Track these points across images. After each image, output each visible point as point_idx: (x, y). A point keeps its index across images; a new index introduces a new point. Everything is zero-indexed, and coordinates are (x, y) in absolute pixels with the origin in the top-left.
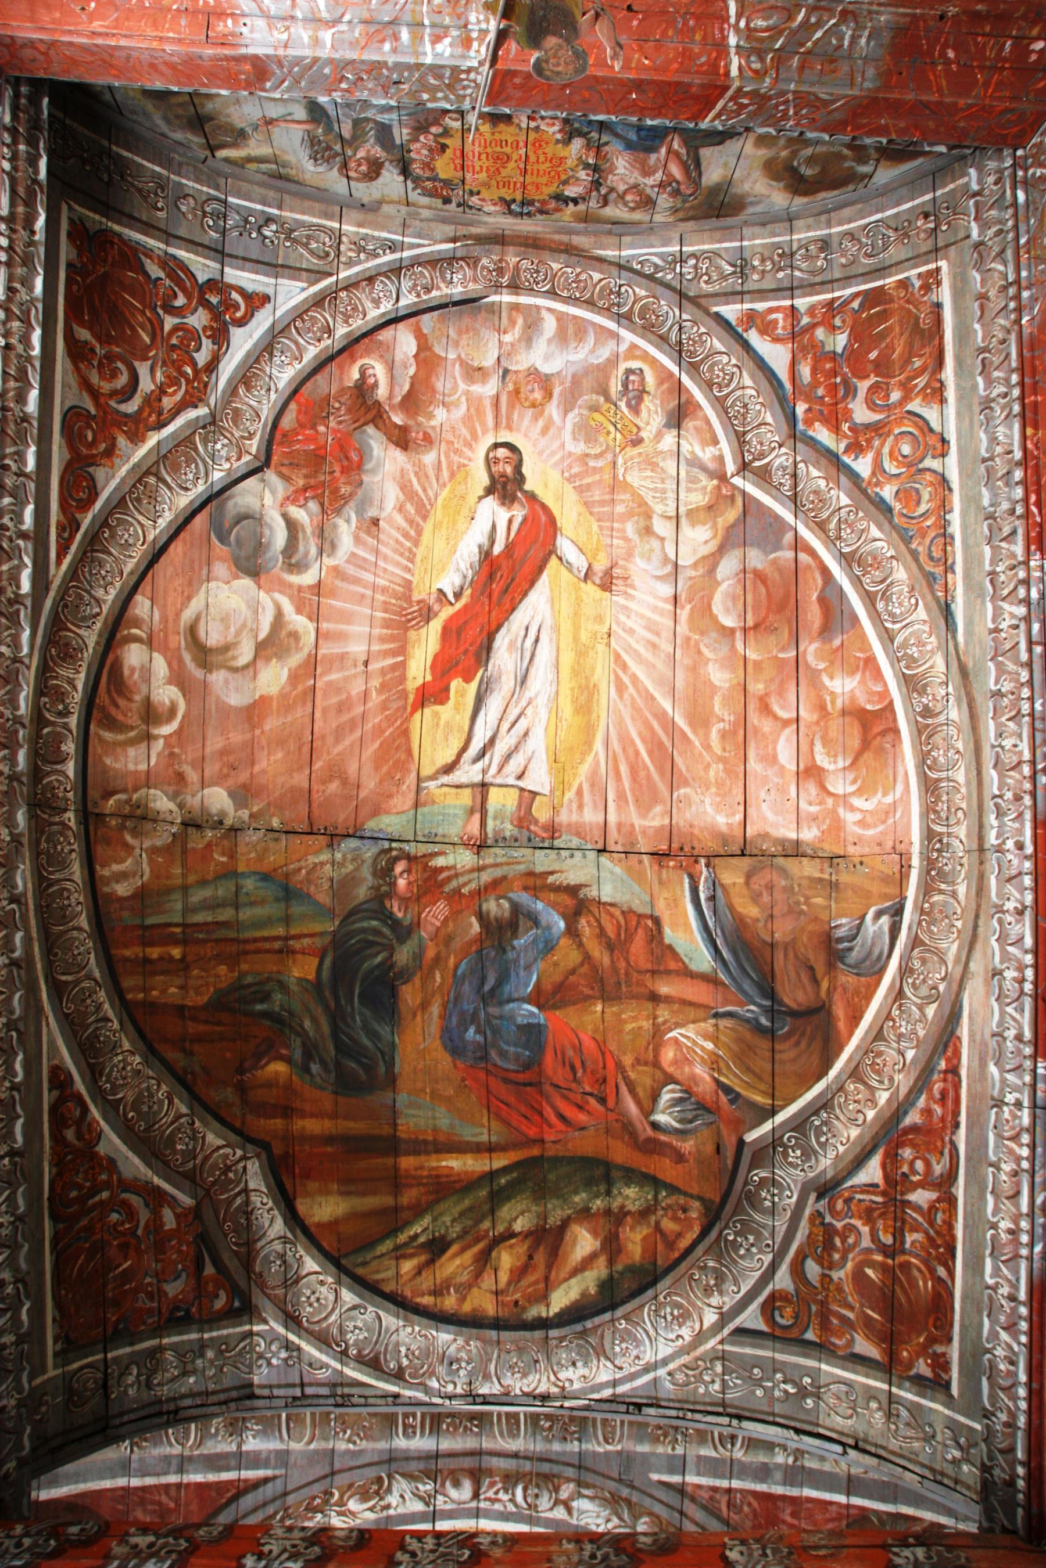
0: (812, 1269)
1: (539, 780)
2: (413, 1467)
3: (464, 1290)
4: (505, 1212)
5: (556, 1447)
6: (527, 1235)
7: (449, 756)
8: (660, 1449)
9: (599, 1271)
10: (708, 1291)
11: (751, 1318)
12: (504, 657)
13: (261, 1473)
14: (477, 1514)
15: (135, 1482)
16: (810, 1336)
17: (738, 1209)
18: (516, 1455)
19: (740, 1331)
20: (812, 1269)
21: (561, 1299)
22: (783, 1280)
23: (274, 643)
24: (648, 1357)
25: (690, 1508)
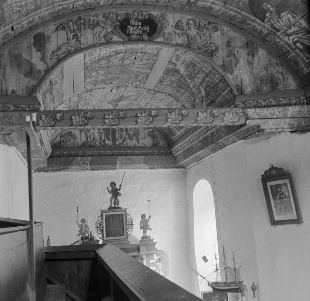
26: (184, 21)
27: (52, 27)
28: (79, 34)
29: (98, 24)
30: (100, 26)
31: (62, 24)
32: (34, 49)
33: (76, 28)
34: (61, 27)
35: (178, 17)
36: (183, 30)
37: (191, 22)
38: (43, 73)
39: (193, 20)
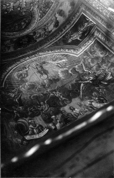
0: (41, 12)
9: (25, 24)
11: (39, 18)
16: (44, 15)
17: (33, 14)
19: (39, 20)
20: (41, 12)
22: (39, 14)
27: (53, 31)
28: (44, 31)
30: (38, 37)
31: (50, 33)
32: (59, 21)
33: (45, 33)
34: (50, 32)
35: (10, 51)
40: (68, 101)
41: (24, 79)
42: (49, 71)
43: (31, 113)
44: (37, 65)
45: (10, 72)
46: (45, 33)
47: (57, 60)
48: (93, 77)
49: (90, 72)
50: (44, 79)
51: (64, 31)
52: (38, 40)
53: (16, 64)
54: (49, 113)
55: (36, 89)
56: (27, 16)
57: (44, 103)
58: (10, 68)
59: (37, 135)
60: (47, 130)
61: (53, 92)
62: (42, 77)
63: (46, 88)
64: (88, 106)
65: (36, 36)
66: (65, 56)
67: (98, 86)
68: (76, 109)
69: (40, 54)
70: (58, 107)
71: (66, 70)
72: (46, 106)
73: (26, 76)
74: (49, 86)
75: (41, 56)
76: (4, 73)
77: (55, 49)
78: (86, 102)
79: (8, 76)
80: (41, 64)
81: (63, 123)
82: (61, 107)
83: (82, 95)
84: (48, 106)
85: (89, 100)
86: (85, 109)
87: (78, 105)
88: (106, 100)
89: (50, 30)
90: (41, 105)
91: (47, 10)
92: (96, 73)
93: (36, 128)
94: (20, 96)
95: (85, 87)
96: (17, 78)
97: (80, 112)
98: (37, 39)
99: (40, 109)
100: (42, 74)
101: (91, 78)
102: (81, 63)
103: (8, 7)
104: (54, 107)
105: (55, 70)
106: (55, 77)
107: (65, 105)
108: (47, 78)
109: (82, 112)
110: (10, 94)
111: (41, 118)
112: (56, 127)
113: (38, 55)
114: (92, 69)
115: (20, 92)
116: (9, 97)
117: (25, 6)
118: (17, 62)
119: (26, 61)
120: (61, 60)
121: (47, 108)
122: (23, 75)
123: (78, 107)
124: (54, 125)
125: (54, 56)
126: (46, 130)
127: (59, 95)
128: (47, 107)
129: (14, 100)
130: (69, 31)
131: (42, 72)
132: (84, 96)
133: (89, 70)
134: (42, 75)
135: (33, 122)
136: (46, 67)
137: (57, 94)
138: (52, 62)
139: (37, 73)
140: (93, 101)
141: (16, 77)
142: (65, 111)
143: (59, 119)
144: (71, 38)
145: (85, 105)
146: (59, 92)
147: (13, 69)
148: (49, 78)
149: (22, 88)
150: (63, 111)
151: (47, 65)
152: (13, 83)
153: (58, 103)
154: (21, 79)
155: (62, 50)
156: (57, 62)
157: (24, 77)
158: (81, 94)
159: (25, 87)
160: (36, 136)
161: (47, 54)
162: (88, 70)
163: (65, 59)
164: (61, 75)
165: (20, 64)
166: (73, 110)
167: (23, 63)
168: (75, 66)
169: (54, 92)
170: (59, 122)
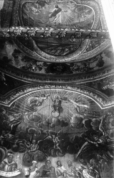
0: (90, 45)
1: (61, 22)
2: (48, 84)
3: (54, 53)
4: (58, 48)
5: (65, 82)
6: (61, 50)
7: (52, 20)
8: (77, 81)
9: (69, 51)
10: (80, 51)
11: (85, 51)
12: (57, 15)
13: (30, 82)
14: (56, 88)
15: (16, 78)
18: (60, 83)
19: (84, 53)
20: (90, 45)
21: (64, 54)
22: (88, 47)
23: (38, 12)
24: (74, 57)
25: (81, 85)
26: (38, 70)
29: (75, 70)
32: (105, 61)
35: (40, 72)
36: (39, 67)
37: (35, 70)
38: (103, 53)
39: (34, 71)
40: (61, 153)
41: (35, 108)
42: (64, 110)
43: (16, 146)
44: (58, 98)
45: (26, 94)
46: (85, 69)
47: (80, 103)
48: (103, 142)
49: (103, 133)
50: (54, 117)
51: (106, 74)
52: (74, 73)
53: (39, 88)
54: (34, 156)
55: (39, 124)
56: (75, 44)
57: (37, 142)
58: (30, 90)
59: (5, 172)
60: (19, 173)
61: (53, 136)
62: (53, 114)
63: (49, 127)
64: (77, 171)
65: (73, 68)
66: (90, 102)
67: (102, 155)
68: (62, 167)
69: (69, 88)
70: (46, 154)
71: (81, 117)
72: (36, 146)
73: (38, 105)
74: (54, 126)
75: (67, 90)
76: (20, 93)
77: (85, 89)
78: (78, 164)
79: (22, 97)
80: (61, 99)
81: (40, 174)
82: (50, 156)
83: (79, 155)
84: (38, 148)
85: (81, 165)
86: (71, 172)
87: (68, 163)
88: (99, 175)
89: (91, 66)
90: (31, 143)
91: (96, 46)
92: (109, 138)
93: (9, 164)
94: (18, 123)
95: (87, 148)
96: (29, 103)
97: (64, 172)
98: (74, 71)
99: (28, 147)
100: (55, 110)
101: (99, 141)
102: (101, 118)
103: (45, 32)
104: (44, 152)
105: (71, 111)
106: (66, 120)
107: (55, 156)
108: (57, 117)
109: (66, 173)
110: (11, 116)
111: (22, 157)
112: (30, 174)
113: (66, 88)
114: (108, 131)
115: (21, 118)
116: (7, 119)
117: (65, 36)
118: (41, 87)
119: (49, 89)
120: (84, 104)
121: (35, 149)
122: (37, 102)
123: (67, 165)
124: (30, 171)
125: (80, 96)
126: (17, 172)
127: (57, 141)
128: (36, 148)
129: (10, 125)
130: (110, 76)
131: (57, 108)
132: (81, 156)
133: (104, 131)
134: (55, 112)
135: (11, 157)
136: (64, 104)
137: (56, 140)
138: (73, 102)
139: (52, 107)
140: (85, 169)
141: (29, 102)
142: (50, 163)
143: (39, 168)
144: (108, 86)
145: (75, 168)
146: (59, 138)
147: (32, 92)
148: (60, 118)
149: (26, 115)
150: (48, 161)
151: (67, 103)
152: (21, 106)
153: (50, 149)
154: (32, 106)
155: (91, 94)
156: (78, 105)
157: (37, 106)
158: (79, 153)
159: (30, 116)
160: (3, 173)
161: (75, 91)
162: (103, 130)
163: (88, 105)
164: (72, 121)
165: (40, 90)
166: (59, 167)
167: (45, 90)
168: (93, 118)
169: (54, 136)
170: (37, 172)
